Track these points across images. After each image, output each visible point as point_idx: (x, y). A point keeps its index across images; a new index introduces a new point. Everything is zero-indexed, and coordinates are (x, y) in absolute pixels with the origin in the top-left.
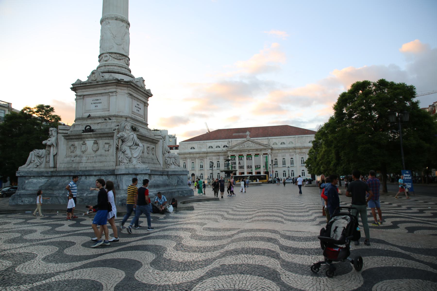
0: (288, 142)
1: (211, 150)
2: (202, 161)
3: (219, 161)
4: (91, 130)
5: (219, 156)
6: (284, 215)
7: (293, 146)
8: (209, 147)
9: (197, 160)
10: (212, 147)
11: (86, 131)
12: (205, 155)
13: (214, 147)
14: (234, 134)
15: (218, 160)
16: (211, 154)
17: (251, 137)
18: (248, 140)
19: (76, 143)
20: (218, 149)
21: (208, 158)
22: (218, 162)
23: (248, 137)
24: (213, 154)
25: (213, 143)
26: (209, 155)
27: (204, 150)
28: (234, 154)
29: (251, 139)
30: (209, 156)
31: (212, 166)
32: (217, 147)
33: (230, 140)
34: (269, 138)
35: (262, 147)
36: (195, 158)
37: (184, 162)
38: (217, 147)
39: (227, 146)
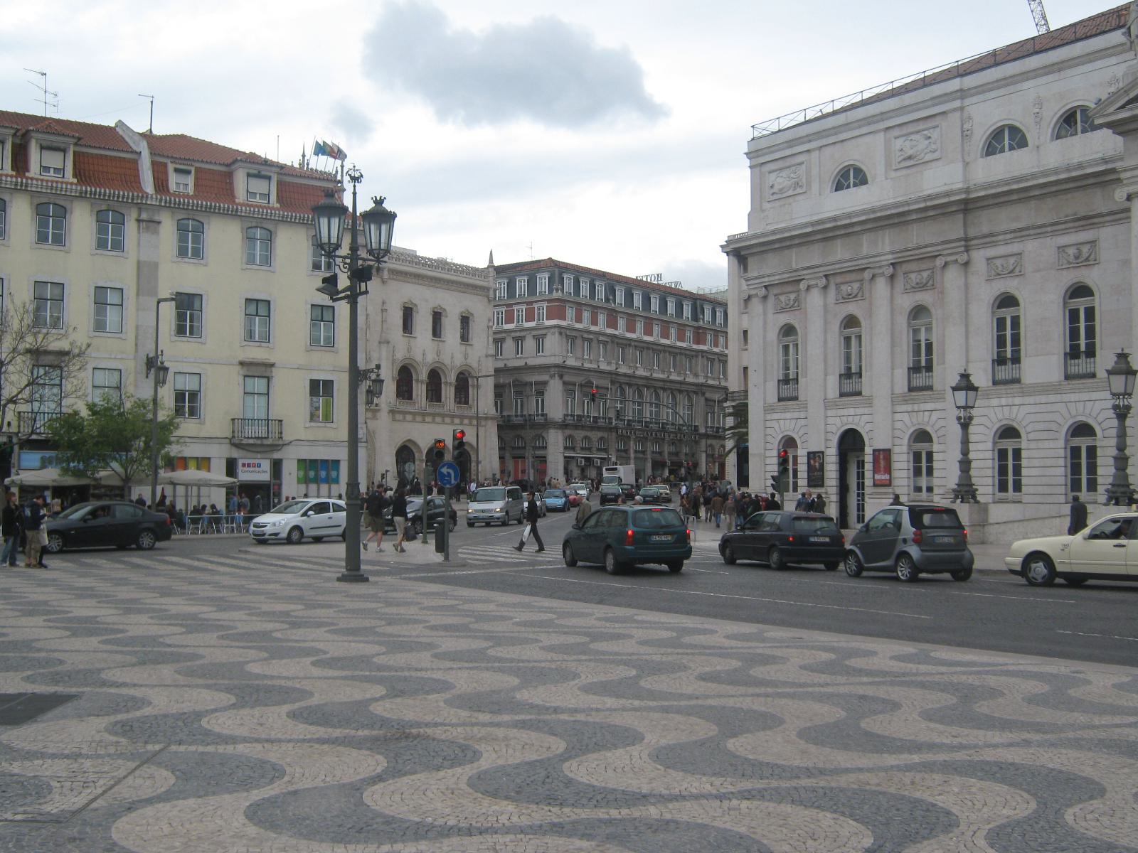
2: (925, 298)
3: (1090, 277)
5: (1088, 221)
9: (881, 286)
12: (953, 229)
13: (1039, 134)
16: (1003, 219)
21: (979, 256)
22: (1081, 290)
24: (1025, 215)
25: (1031, 89)
26: (985, 222)
27: (942, 178)
30: (989, 239)
36: (860, 271)
37: (784, 319)
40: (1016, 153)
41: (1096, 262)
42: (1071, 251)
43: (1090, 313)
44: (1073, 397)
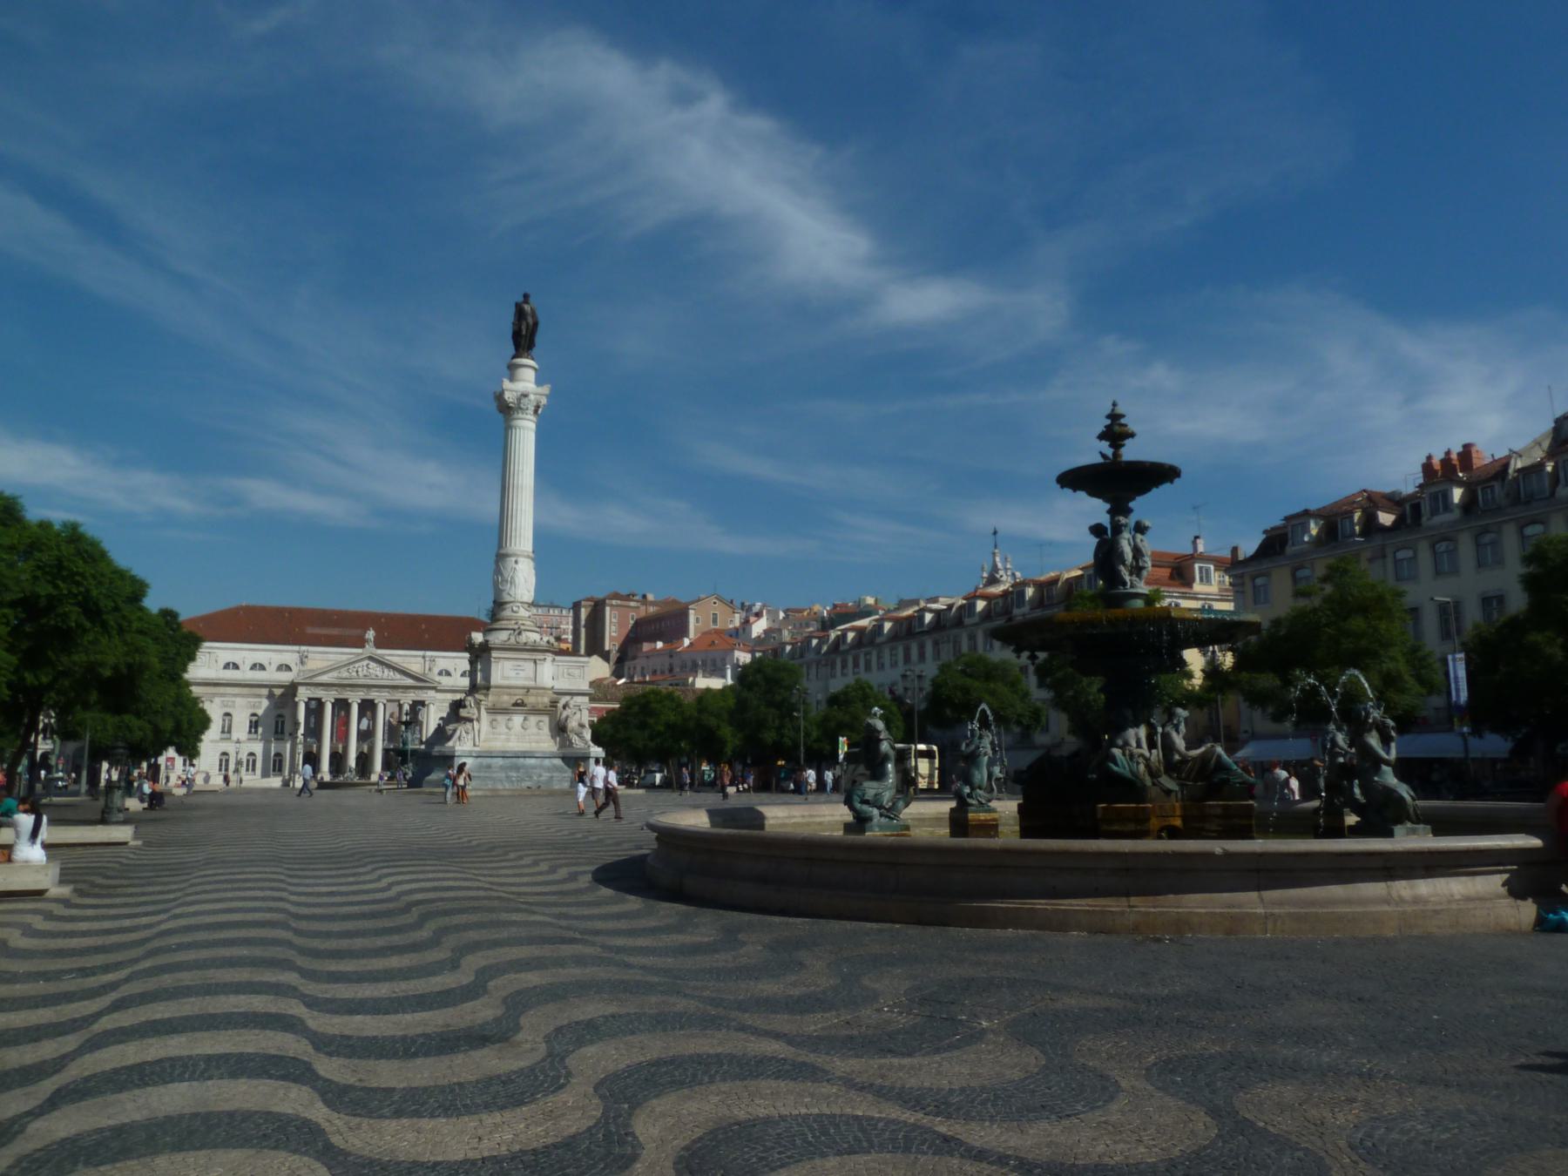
1: (231, 675)
4: (523, 704)
6: (297, 932)
8: (227, 666)
10: (236, 667)
11: (516, 704)
14: (310, 630)
17: (378, 645)
18: (371, 658)
19: (500, 718)
20: (259, 676)
21: (217, 700)
23: (370, 649)
26: (222, 690)
29: (380, 652)
31: (227, 730)
32: (254, 667)
33: (304, 648)
34: (429, 653)
35: (410, 682)
38: (254, 667)
39: (288, 668)
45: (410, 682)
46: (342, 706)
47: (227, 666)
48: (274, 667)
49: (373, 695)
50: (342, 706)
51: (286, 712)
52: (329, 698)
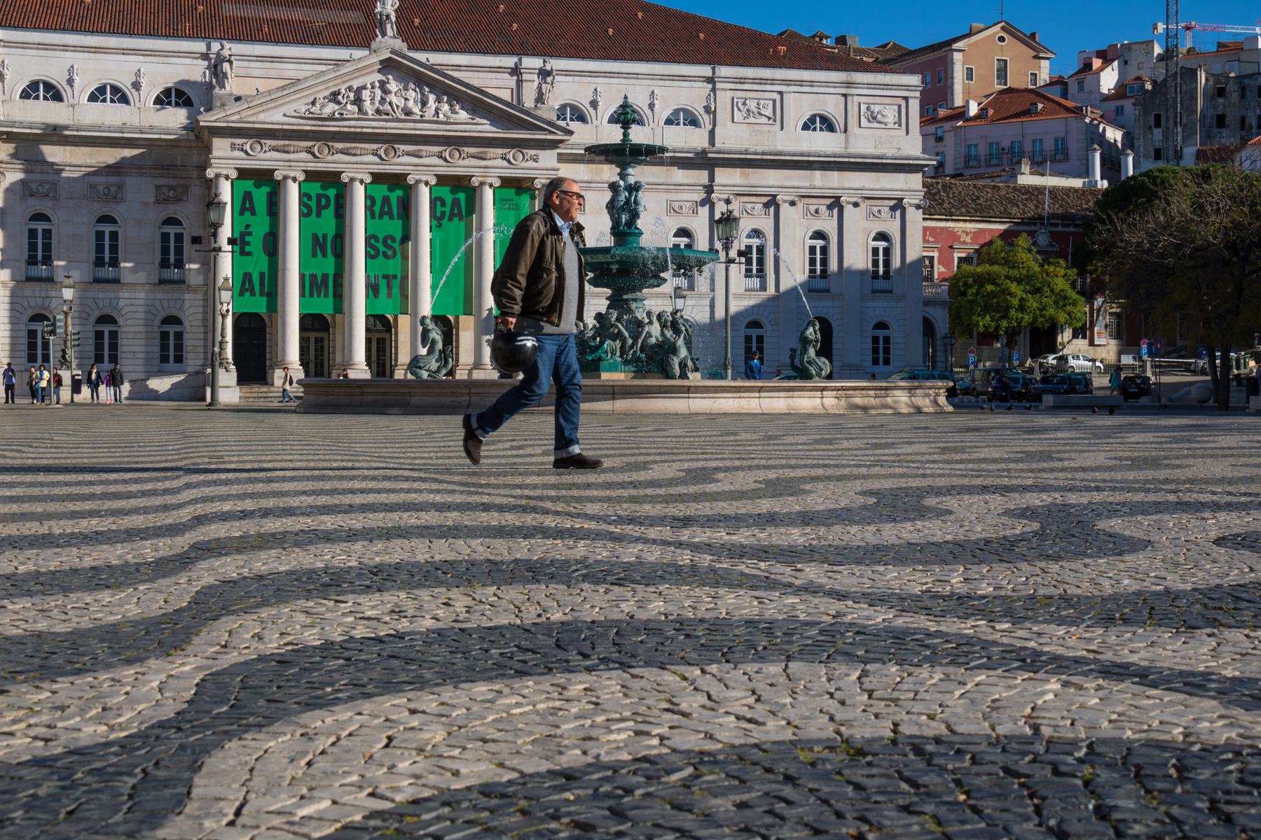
0: (664, 112)
7: (693, 139)
8: (30, 91)
14: (229, 10)
15: (101, 209)
20: (110, 116)
23: (389, 42)
28: (265, 157)
32: (97, 95)
38: (97, 95)
40: (52, 104)
41: (123, 200)
42: (101, 189)
43: (114, 236)
44: (101, 295)
45: (485, 128)
46: (328, 192)
47: (30, 91)
48: (150, 92)
49: (401, 162)
50: (328, 192)
51: (187, 212)
52: (290, 165)
